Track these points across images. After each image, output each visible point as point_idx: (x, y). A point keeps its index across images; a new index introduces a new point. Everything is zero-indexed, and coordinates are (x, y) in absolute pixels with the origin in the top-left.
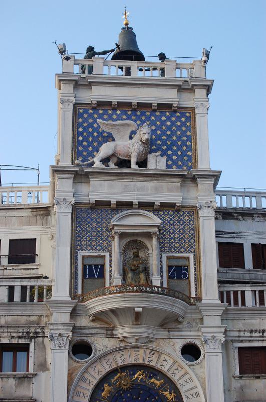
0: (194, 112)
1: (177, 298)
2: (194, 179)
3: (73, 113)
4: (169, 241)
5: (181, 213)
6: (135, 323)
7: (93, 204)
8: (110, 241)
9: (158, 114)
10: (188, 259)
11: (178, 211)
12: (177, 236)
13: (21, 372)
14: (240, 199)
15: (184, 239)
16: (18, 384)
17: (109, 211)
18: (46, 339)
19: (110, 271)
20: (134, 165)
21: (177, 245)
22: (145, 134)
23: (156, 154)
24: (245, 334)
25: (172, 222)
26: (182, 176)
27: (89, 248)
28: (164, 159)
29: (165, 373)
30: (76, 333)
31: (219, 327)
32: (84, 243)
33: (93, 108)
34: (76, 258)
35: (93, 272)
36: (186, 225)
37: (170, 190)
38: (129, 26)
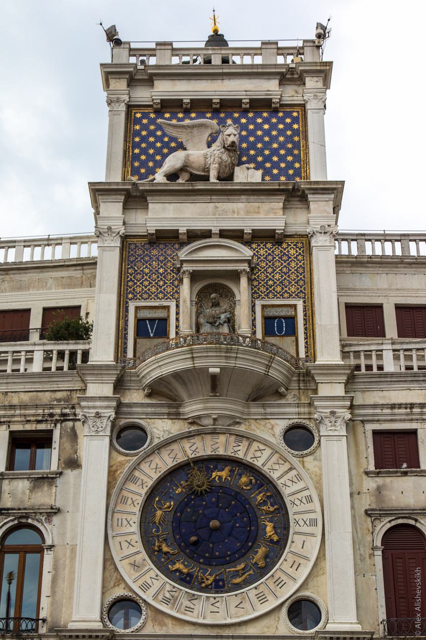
5: (284, 245)
7: (153, 234)
8: (178, 285)
9: (251, 115)
10: (295, 306)
11: (279, 243)
12: (277, 276)
13: (39, 472)
15: (288, 280)
17: (177, 246)
18: (78, 424)
19: (177, 327)
21: (279, 289)
22: (229, 135)
25: (270, 258)
27: (145, 296)
28: (259, 173)
31: (342, 398)
32: (138, 290)
34: (127, 311)
35: (153, 328)
36: (291, 261)
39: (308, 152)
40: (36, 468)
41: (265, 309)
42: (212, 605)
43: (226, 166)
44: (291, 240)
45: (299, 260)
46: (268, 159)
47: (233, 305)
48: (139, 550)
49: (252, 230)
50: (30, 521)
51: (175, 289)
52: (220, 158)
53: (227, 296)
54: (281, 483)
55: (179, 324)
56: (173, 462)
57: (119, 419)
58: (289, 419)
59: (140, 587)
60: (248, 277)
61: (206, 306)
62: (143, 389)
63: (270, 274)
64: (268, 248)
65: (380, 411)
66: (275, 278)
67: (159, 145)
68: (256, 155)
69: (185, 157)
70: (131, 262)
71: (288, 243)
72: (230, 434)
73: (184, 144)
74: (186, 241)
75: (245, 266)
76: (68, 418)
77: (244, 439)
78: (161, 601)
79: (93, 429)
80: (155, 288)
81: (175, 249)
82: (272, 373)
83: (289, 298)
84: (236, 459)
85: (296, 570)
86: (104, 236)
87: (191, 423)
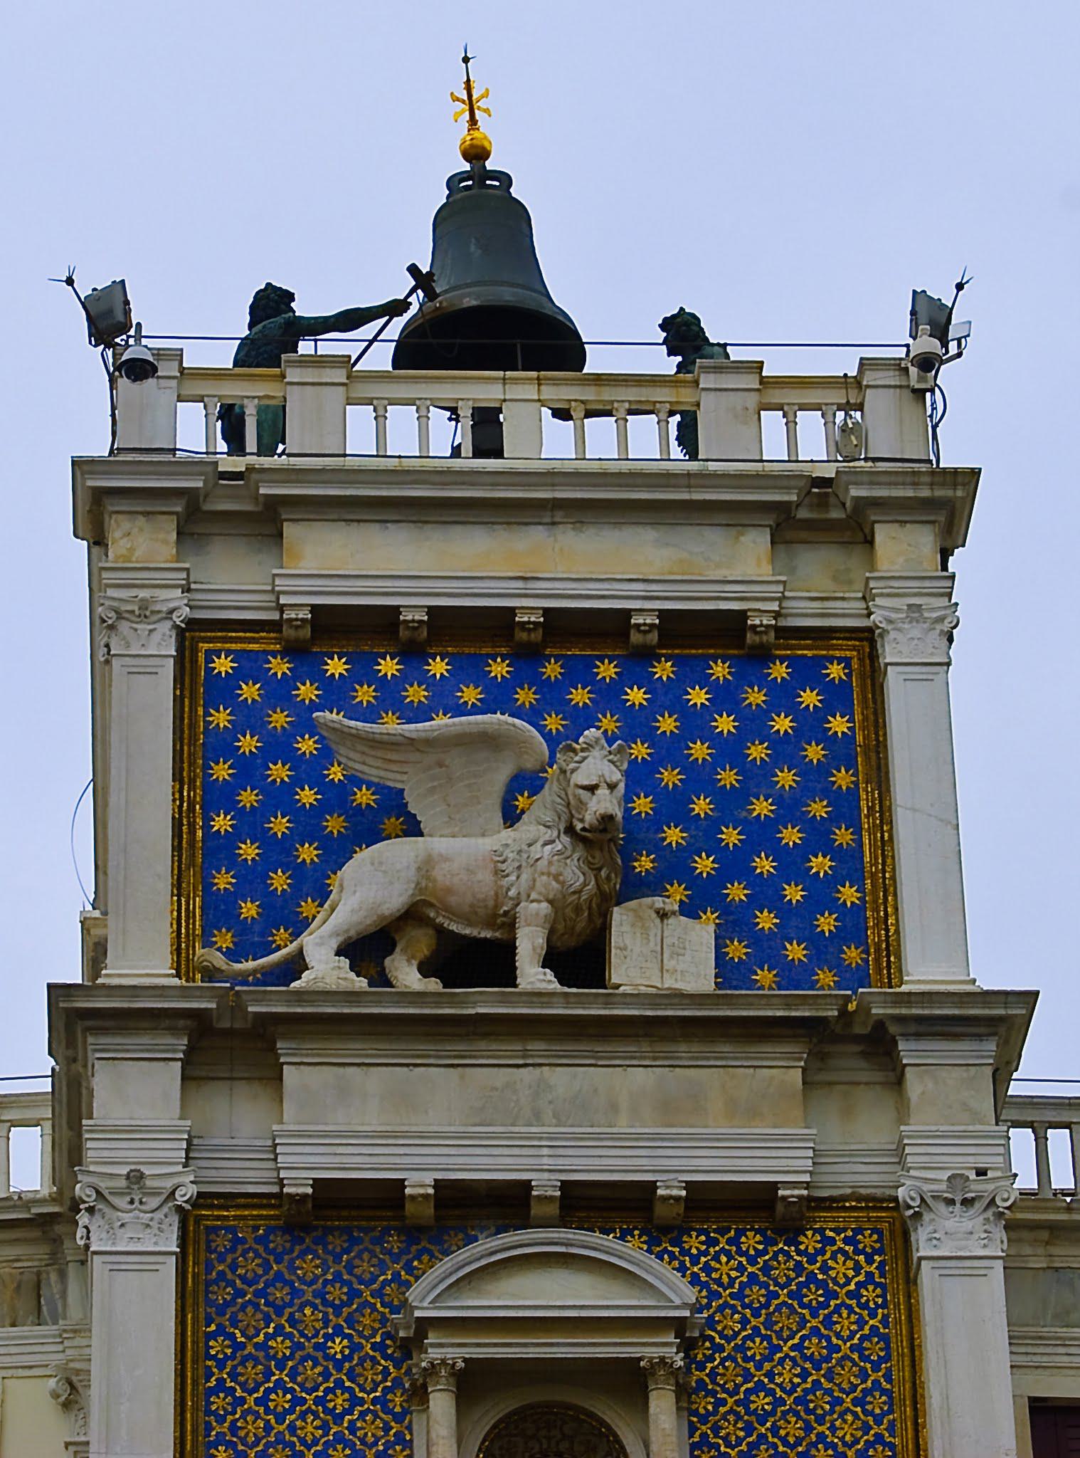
0: (873, 656)
3: (179, 679)
5: (809, 1241)
8: (406, 1412)
9: (664, 670)
12: (786, 1375)
15: (829, 1392)
17: (394, 1242)
20: (533, 974)
22: (592, 789)
23: (658, 902)
28: (703, 932)
33: (292, 651)
36: (837, 1310)
38: (490, 165)
45: (865, 1306)
46: (735, 865)
49: (689, 1185)
52: (556, 877)
60: (677, 1384)
63: (759, 1367)
64: (745, 1254)
66: (778, 1380)
67: (307, 796)
68: (691, 850)
69: (419, 869)
70: (218, 1306)
71: (821, 1231)
73: (408, 797)
81: (389, 1252)
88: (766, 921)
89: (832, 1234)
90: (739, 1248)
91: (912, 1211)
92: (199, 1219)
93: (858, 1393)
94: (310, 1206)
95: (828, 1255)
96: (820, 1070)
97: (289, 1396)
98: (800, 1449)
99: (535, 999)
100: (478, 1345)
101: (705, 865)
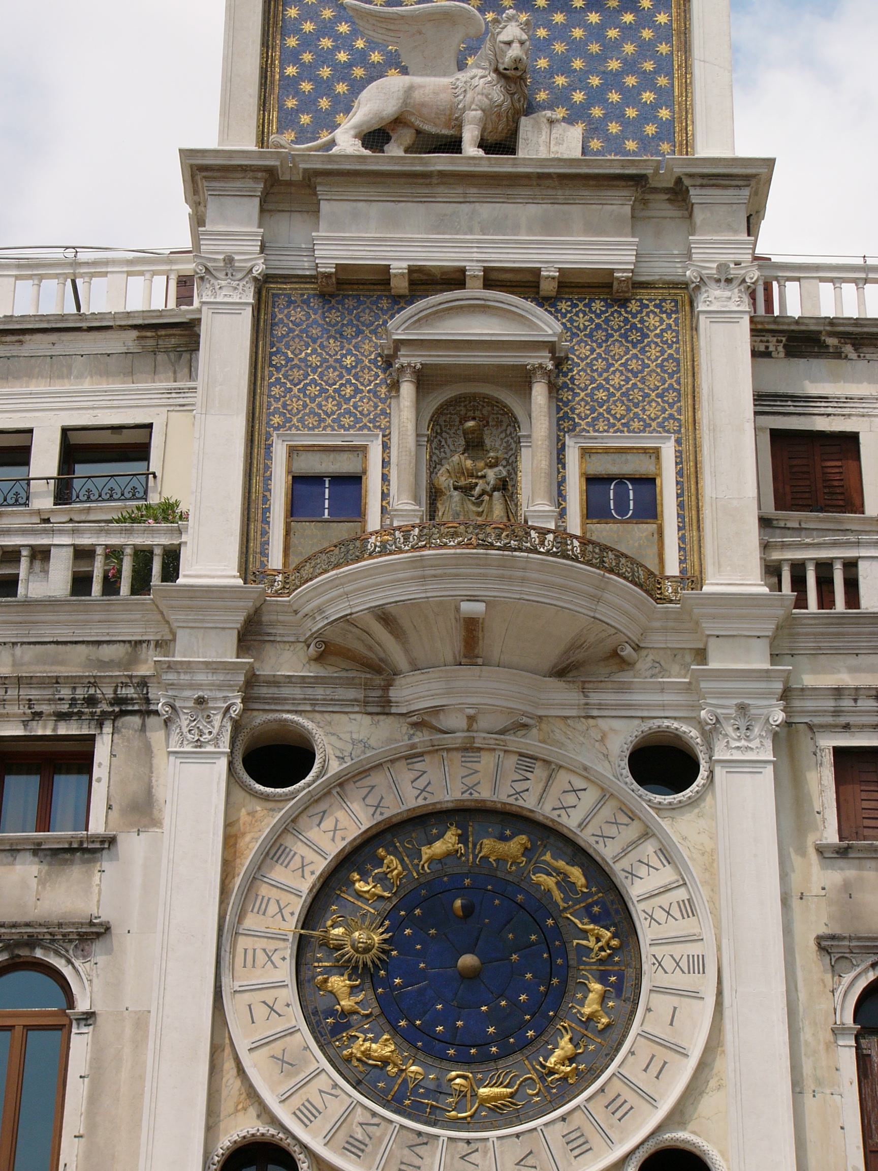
1: (611, 571)
2: (678, 193)
4: (591, 395)
5: (633, 306)
6: (463, 661)
12: (616, 380)
13: (60, 834)
14: (849, 289)
15: (641, 390)
16: (48, 873)
17: (384, 304)
18: (152, 721)
19: (385, 496)
21: (620, 410)
22: (509, 43)
24: (860, 703)
26: (637, 181)
27: (311, 421)
28: (575, 133)
29: (571, 835)
30: (257, 699)
32: (295, 405)
36: (648, 345)
37: (591, 228)
39: (691, 83)
40: (51, 828)
41: (587, 456)
42: (462, 1158)
43: (499, 115)
44: (649, 294)
45: (666, 342)
46: (596, 96)
47: (513, 446)
48: (294, 1023)
49: (560, 270)
50: (39, 953)
51: (381, 406)
52: (487, 97)
53: (499, 423)
54: (623, 870)
55: (388, 490)
56: (373, 815)
57: (249, 713)
58: (642, 718)
59: (294, 1113)
60: (550, 382)
61: (452, 447)
62: (305, 642)
63: (600, 375)
64: (594, 312)
65: (852, 703)
66: (612, 383)
68: (571, 88)
72: (505, 751)
74: (406, 292)
75: (542, 357)
76: (130, 708)
77: (539, 764)
78: (344, 1148)
79: (189, 736)
80: (335, 402)
82: (604, 612)
83: (644, 431)
84: (518, 809)
85: (657, 1077)
86: (216, 278)
87: (415, 725)
88: (614, 128)
89: (646, 302)
90: (590, 309)
91: (694, 285)
92: (268, 290)
93: (660, 391)
94: (334, 280)
95: (644, 314)
96: (643, 209)
97: (318, 388)
98: (623, 421)
99: (471, 162)
100: (430, 356)
101: (578, 97)
